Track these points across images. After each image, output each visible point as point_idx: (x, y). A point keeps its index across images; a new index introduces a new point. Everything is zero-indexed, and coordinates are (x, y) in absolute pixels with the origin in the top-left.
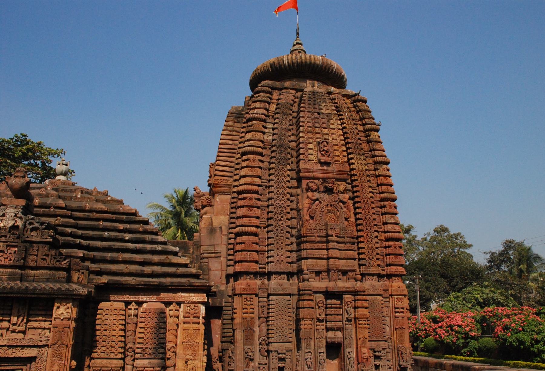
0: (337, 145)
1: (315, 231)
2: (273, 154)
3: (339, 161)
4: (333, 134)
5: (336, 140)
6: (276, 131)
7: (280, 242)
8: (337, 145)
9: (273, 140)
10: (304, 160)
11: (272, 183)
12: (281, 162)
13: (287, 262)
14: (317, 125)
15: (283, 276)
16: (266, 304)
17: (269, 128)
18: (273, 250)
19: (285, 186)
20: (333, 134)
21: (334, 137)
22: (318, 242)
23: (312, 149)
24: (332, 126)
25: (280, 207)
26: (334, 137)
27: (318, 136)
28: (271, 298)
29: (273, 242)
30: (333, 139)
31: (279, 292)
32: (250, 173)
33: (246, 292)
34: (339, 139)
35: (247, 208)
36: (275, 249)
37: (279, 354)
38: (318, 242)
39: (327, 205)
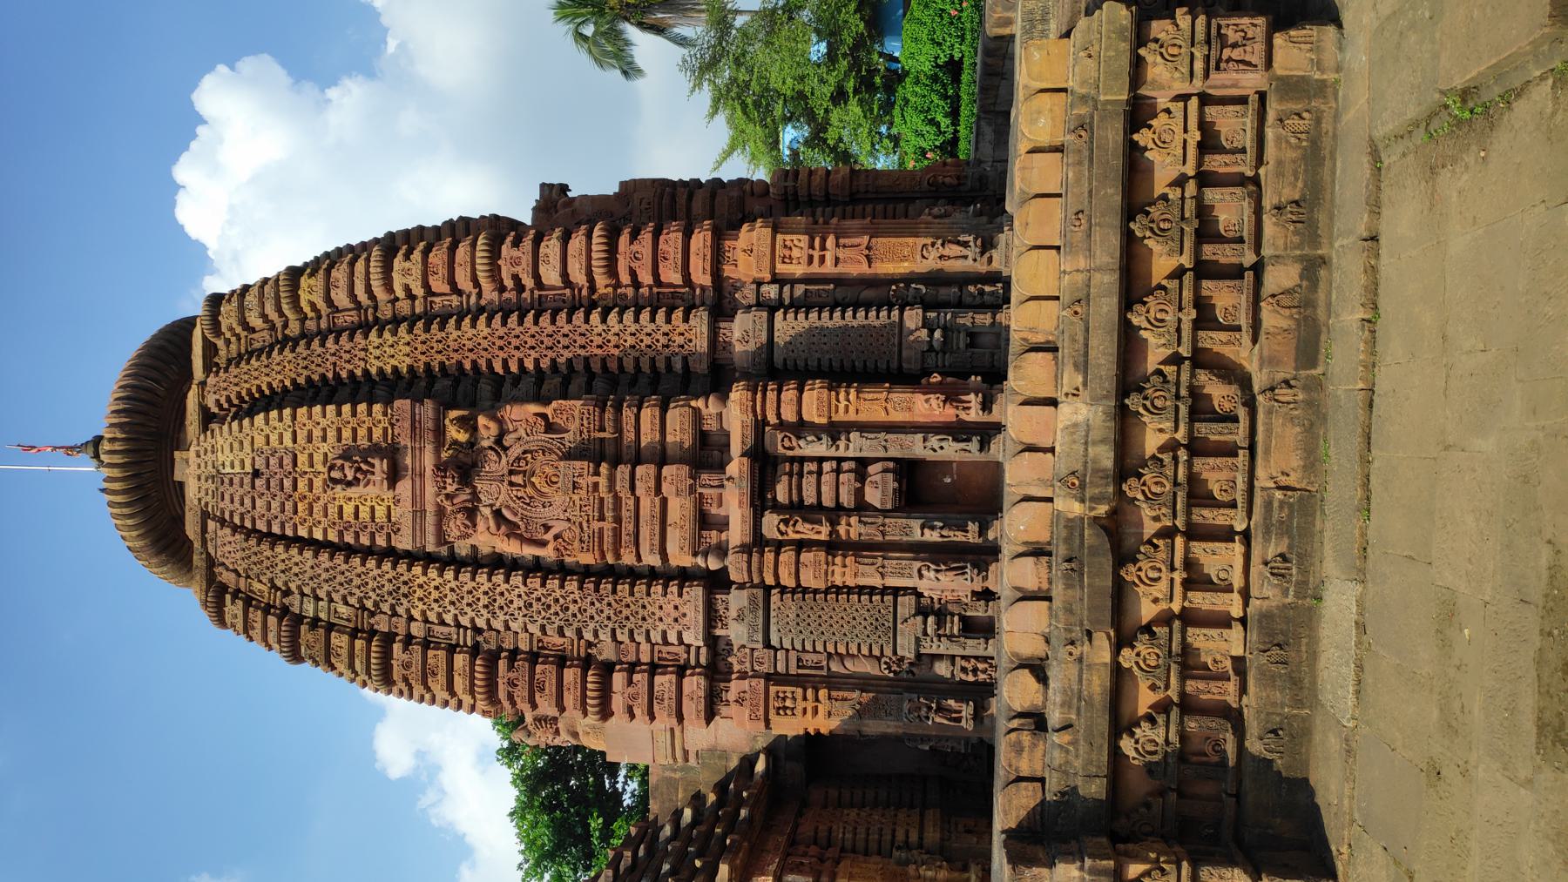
0: (339, 430)
1: (585, 525)
2: (385, 607)
3: (385, 429)
4: (310, 439)
5: (324, 430)
6: (322, 594)
7: (626, 612)
8: (339, 430)
9: (346, 603)
10: (389, 536)
11: (465, 621)
12: (404, 589)
13: (680, 595)
14: (287, 483)
15: (720, 607)
16: (793, 656)
17: (316, 610)
18: (648, 632)
19: (471, 585)
20: (310, 439)
21: (317, 433)
22: (618, 519)
23: (357, 508)
24: (288, 441)
25: (529, 605)
26: (317, 433)
27: (318, 483)
28: (774, 642)
29: (626, 630)
30: (324, 439)
31: (760, 621)
32: (442, 677)
33: (762, 709)
34: (324, 423)
35: (537, 695)
36: (645, 626)
37: (925, 634)
38: (618, 519)
39: (511, 484)
